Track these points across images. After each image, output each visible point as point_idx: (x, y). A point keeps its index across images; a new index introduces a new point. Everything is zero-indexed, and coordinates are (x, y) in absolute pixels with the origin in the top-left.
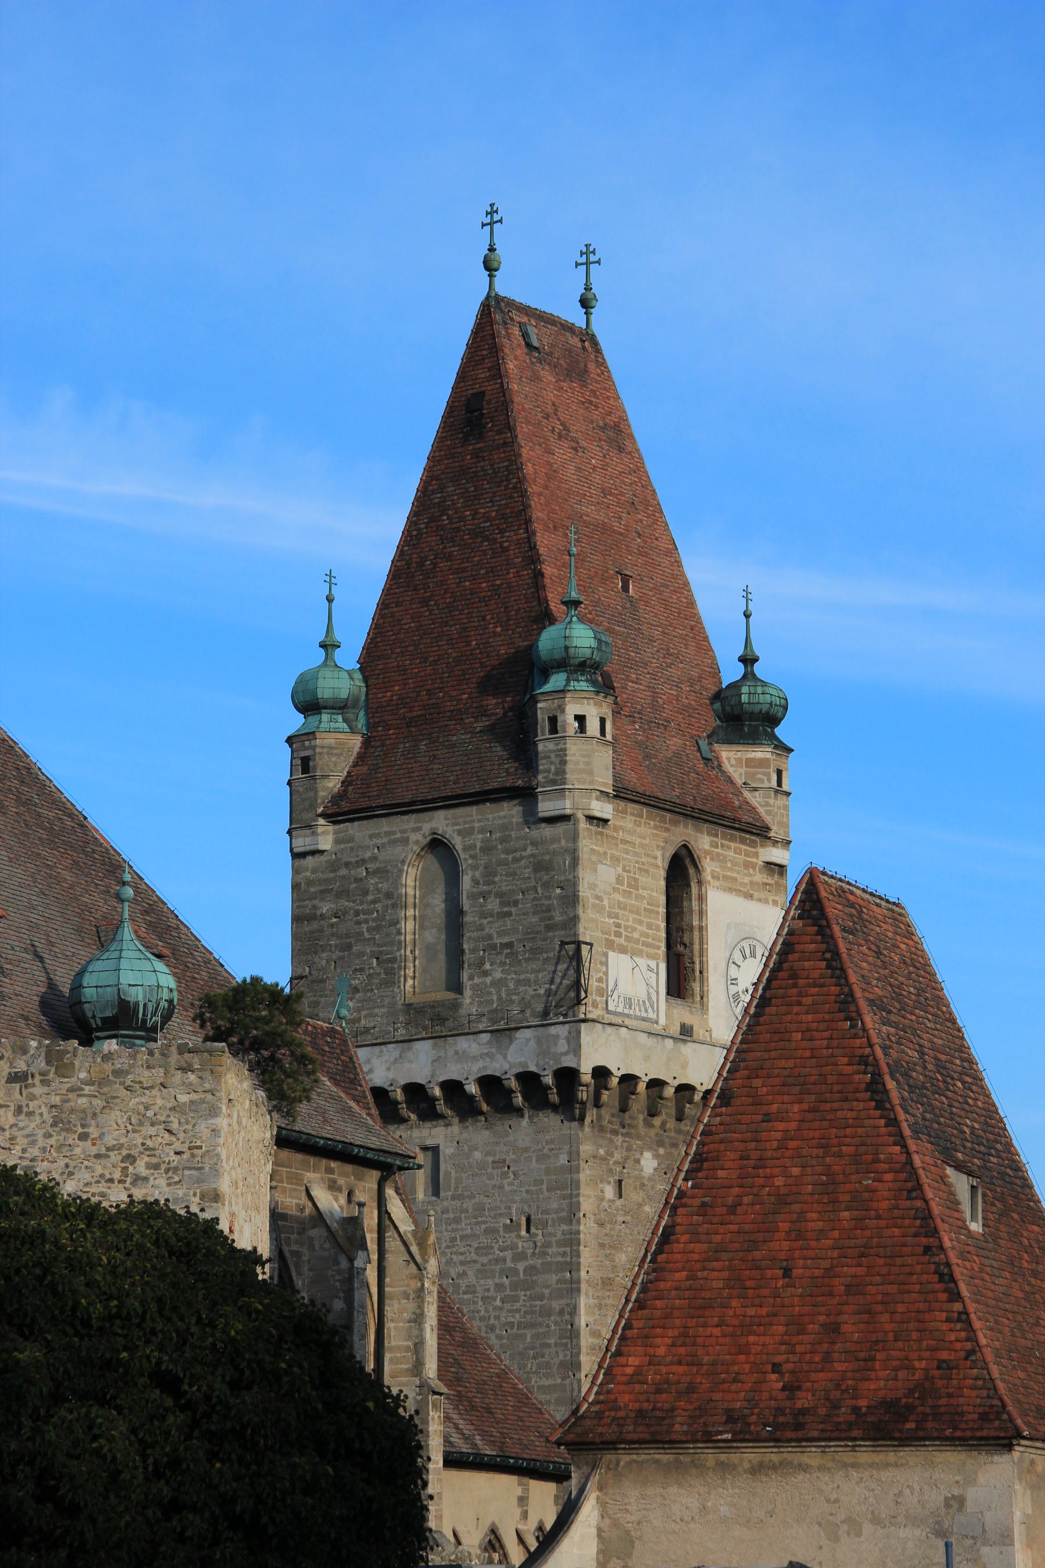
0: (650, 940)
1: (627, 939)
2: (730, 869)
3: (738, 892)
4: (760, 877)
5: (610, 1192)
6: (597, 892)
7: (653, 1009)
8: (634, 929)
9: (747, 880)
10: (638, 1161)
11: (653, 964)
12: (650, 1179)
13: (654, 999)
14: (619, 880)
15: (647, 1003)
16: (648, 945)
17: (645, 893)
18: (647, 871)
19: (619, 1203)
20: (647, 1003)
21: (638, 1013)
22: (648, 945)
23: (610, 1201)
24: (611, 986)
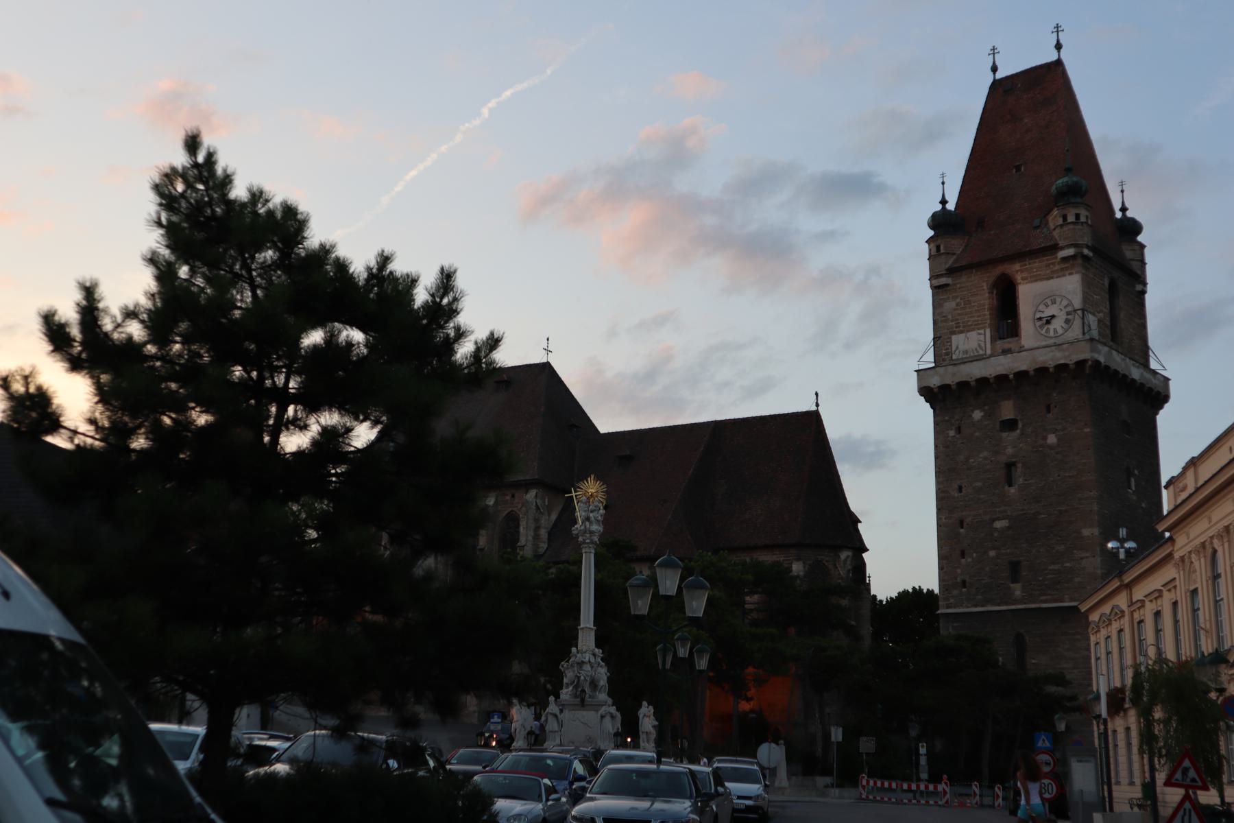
0: (980, 322)
1: (964, 327)
2: (1037, 271)
3: (1042, 279)
4: (1057, 267)
5: (952, 433)
6: (944, 315)
7: (982, 349)
8: (968, 321)
9: (1048, 272)
10: (971, 416)
11: (982, 331)
12: (978, 421)
13: (983, 345)
14: (957, 305)
15: (978, 349)
16: (980, 324)
17: (976, 304)
18: (977, 294)
19: (958, 436)
20: (978, 349)
21: (972, 354)
22: (980, 324)
23: (952, 437)
24: (954, 348)
